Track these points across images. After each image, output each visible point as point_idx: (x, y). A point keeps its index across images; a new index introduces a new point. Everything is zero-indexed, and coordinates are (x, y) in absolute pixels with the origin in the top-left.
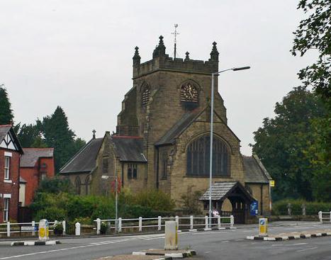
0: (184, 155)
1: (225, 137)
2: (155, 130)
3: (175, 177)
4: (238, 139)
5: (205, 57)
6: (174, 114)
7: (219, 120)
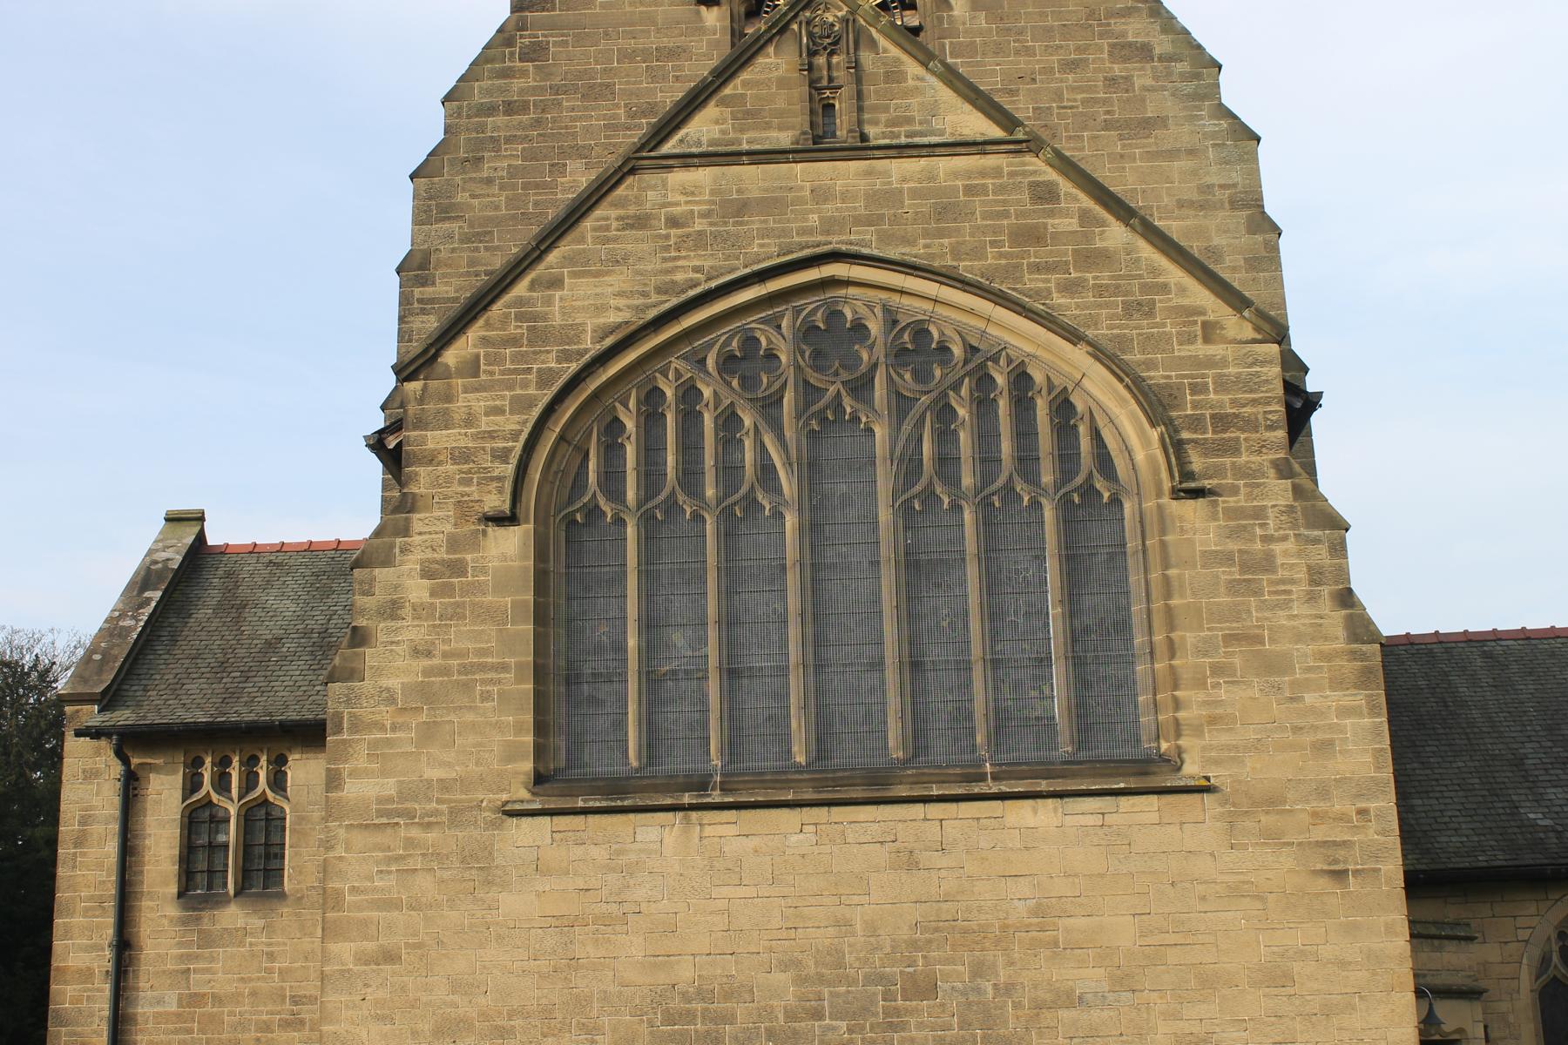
1: (1067, 306)
3: (389, 815)
7: (977, 125)
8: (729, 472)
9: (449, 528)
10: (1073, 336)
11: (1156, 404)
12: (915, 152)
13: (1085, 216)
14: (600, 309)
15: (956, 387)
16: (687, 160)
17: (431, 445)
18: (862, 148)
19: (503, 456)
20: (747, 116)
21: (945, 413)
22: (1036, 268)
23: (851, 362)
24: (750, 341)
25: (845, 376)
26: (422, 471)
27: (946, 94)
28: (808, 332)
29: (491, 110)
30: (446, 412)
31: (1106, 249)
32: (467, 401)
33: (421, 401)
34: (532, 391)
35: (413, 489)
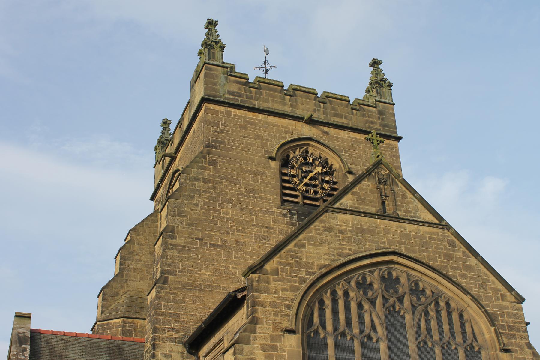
0: (293, 342)
2: (188, 287)
4: (510, 289)
5: (356, 89)
6: (258, 237)
8: (361, 323)
9: (270, 332)
10: (466, 292)
11: (492, 320)
12: (414, 223)
13: (464, 253)
14: (319, 258)
15: (430, 304)
16: (344, 211)
17: (262, 299)
18: (397, 219)
19: (289, 307)
20: (361, 200)
21: (427, 313)
22: (452, 268)
23: (397, 292)
24: (364, 278)
25: (396, 295)
26: (260, 308)
27: (420, 206)
28: (383, 278)
29: (197, 180)
30: (267, 287)
31: (471, 265)
32: (273, 285)
33: (258, 282)
34: (297, 284)
35: (257, 315)
